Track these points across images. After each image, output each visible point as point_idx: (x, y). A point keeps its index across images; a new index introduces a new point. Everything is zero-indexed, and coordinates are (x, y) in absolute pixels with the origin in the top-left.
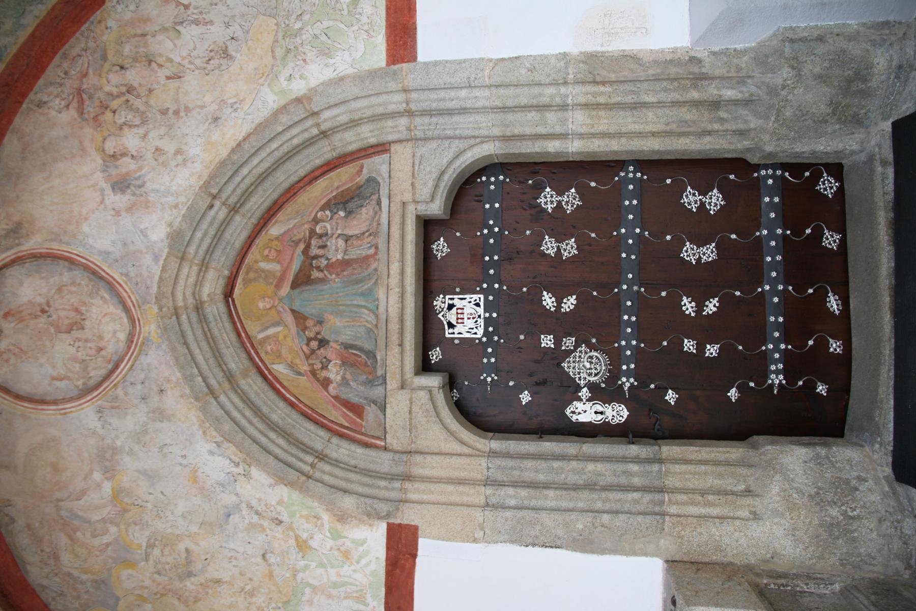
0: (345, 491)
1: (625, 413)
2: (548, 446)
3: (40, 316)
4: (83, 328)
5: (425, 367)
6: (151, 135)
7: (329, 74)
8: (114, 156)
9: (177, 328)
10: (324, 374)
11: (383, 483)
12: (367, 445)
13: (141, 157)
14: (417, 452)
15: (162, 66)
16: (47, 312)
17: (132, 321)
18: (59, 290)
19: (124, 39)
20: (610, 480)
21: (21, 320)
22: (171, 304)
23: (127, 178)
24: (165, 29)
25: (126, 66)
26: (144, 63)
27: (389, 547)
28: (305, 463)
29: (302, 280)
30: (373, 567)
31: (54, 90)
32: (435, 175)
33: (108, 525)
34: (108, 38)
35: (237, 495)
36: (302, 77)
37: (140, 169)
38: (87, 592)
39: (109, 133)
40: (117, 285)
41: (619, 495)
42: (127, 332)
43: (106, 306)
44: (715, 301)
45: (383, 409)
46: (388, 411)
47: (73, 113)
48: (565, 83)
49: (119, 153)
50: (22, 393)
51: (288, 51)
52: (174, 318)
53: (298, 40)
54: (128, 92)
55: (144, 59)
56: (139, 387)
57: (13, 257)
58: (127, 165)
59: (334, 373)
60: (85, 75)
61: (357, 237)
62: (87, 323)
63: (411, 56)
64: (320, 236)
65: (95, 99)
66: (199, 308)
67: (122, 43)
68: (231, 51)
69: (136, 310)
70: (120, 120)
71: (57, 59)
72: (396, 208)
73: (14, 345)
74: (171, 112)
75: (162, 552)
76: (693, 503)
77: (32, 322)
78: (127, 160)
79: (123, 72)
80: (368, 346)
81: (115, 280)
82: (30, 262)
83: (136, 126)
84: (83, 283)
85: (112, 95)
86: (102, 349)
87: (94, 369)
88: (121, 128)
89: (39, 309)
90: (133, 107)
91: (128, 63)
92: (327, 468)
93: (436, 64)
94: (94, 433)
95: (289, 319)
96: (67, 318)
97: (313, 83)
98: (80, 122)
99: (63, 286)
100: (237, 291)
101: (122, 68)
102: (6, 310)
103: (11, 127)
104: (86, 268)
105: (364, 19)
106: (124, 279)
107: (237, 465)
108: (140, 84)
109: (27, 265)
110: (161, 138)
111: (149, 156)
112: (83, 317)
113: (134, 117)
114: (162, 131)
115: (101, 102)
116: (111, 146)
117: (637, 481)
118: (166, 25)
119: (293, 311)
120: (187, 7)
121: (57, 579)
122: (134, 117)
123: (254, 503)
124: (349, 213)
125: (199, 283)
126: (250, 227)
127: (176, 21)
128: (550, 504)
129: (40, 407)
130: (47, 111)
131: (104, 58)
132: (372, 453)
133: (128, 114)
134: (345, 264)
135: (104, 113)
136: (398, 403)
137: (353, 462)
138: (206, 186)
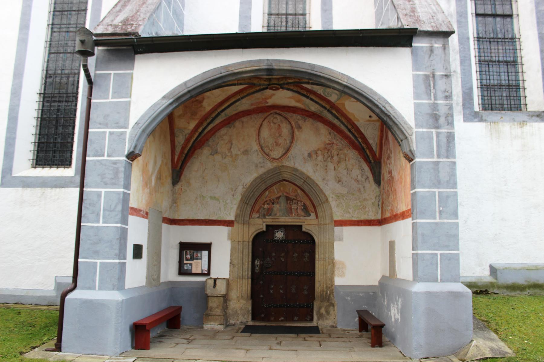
0: (241, 211)
1: (257, 272)
2: (250, 255)
4: (276, 146)
5: (267, 226)
6: (321, 163)
7: (333, 206)
10: (266, 204)
11: (243, 219)
12: (250, 214)
14: (249, 226)
17: (278, 159)
18: (285, 140)
20: (244, 268)
24: (346, 165)
27: (229, 221)
28: (246, 201)
29: (288, 199)
30: (225, 217)
32: (311, 230)
35: (239, 186)
36: (332, 200)
41: (241, 269)
44: (283, 292)
45: (258, 218)
46: (258, 219)
47: (328, 142)
48: (329, 259)
50: (261, 130)
51: (339, 197)
53: (341, 199)
58: (314, 156)
59: (266, 206)
60: (337, 145)
61: (297, 212)
62: (277, 147)
63: (335, 226)
64: (298, 203)
66: (281, 174)
68: (340, 182)
71: (341, 137)
72: (304, 220)
76: (240, 285)
80: (272, 214)
88: (323, 155)
92: (245, 206)
93: (334, 231)
95: (278, 195)
97: (331, 203)
100: (285, 182)
101: (338, 155)
102: (281, 125)
104: (290, 146)
105: (345, 215)
107: (246, 186)
110: (320, 166)
116: (319, 152)
117: (244, 273)
119: (280, 196)
120: (351, 171)
123: (237, 189)
124: (302, 210)
125: (286, 174)
126: (300, 185)
128: (239, 255)
131: (341, 150)
132: (249, 216)
134: (291, 209)
136: (259, 221)
137: (246, 211)
138: (308, 177)
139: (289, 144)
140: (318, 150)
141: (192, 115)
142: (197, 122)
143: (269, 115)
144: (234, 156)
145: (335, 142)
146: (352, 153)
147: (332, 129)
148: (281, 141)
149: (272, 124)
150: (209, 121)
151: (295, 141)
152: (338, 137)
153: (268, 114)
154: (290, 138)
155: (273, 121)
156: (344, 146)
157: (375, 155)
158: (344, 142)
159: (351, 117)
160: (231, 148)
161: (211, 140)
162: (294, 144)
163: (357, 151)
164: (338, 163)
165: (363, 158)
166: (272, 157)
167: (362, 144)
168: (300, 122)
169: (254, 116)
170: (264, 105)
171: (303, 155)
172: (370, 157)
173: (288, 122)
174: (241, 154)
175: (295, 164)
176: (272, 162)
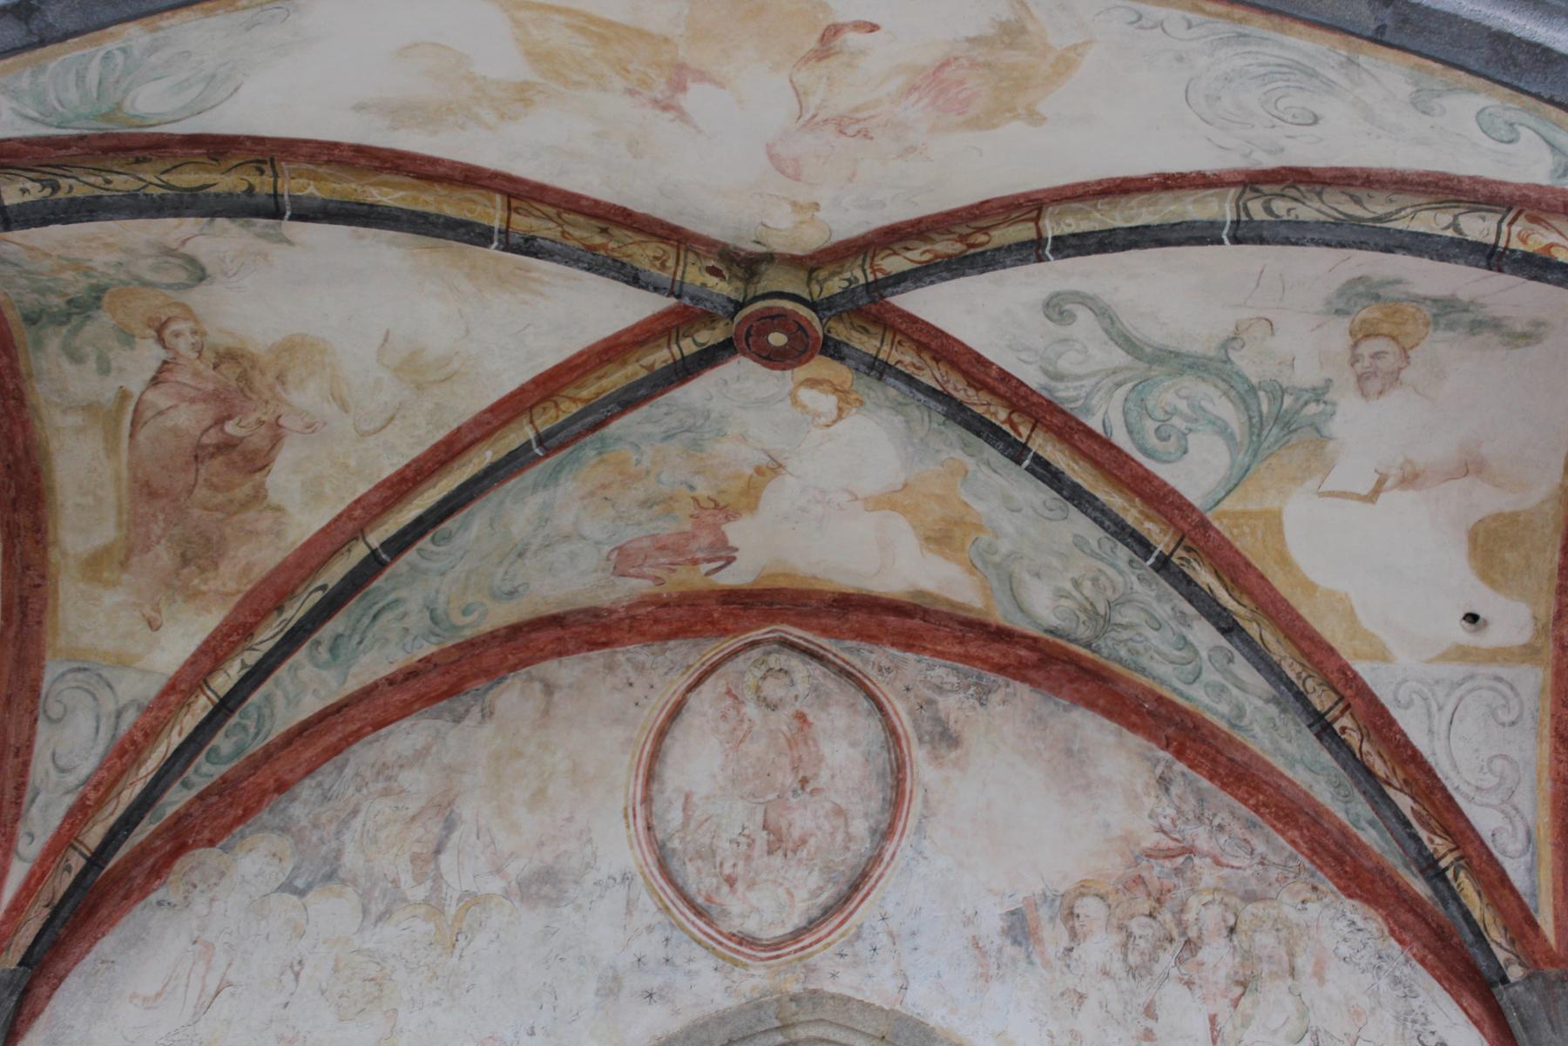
3: (796, 776)
4: (770, 852)
6: (1107, 985)
8: (1071, 914)
9: (759, 1029)
13: (1069, 966)
15: (1236, 1006)
16: (803, 788)
17: (777, 945)
18: (839, 812)
19: (1284, 933)
21: (792, 743)
22: (802, 1018)
23: (1032, 941)
24: (1304, 1011)
25: (1234, 937)
26: (1241, 972)
31: (1190, 805)
33: (429, 883)
34: (1287, 906)
37: (1047, 964)
38: (322, 841)
39: (1114, 905)
40: (837, 921)
42: (757, 935)
43: (806, 896)
47: (1152, 839)
49: (1077, 924)
50: (668, 741)
52: (777, 1024)
54: (1188, 942)
55: (1248, 973)
56: (661, 954)
57: (900, 731)
58: (1054, 936)
60: (1218, 863)
62: (777, 860)
65: (1175, 880)
67: (1278, 930)
69: (796, 951)
70: (1134, 926)
71: (1244, 811)
73: (750, 730)
74: (1150, 1023)
75: (372, 980)
77: (785, 761)
78: (1065, 941)
79: (1225, 932)
81: (851, 913)
82: (890, 759)
83: (1126, 955)
84: (849, 855)
85: (1182, 911)
86: (731, 886)
87: (699, 871)
88: (1121, 928)
89: (809, 774)
90: (1161, 952)
91: (1240, 942)
94: (588, 866)
96: (790, 825)
98: (1132, 852)
99: (846, 820)
101: (1232, 930)
102: (810, 718)
103: (1125, 731)
104: (876, 859)
106: (852, 932)
108: (1203, 964)
109: (885, 755)
110: (1103, 1005)
111: (1070, 981)
112: (790, 854)
113: (1142, 953)
114: (1116, 1008)
115: (1169, 891)
116: (1090, 908)
118: (1311, 1014)
121: (351, 791)
122: (1142, 953)
127: (1321, 1035)
129: (641, 772)
130: (1153, 793)
131: (1250, 897)
133: (1147, 941)
135: (1149, 895)
139: (864, 846)
140: (1083, 890)
141: (185, 561)
142: (209, 621)
143: (734, 654)
144: (452, 910)
145: (1201, 837)
146: (1341, 925)
147: (1180, 754)
148: (803, 818)
149: (751, 710)
150: (295, 611)
151: (912, 822)
152: (1224, 803)
153: (731, 644)
154: (875, 805)
155: (758, 689)
156: (1274, 873)
157: (1535, 926)
158: (1274, 845)
159: (1330, 629)
160: (438, 851)
161: (307, 790)
162: (902, 847)
163: (1371, 912)
164: (1238, 990)
165: (1422, 962)
166: (735, 925)
167: (1423, 834)
168: (950, 705)
169: (633, 655)
170: (697, 578)
171: (968, 922)
172: (1495, 935)
173: (865, 704)
174: (507, 894)
175: (903, 988)
176: (735, 963)
